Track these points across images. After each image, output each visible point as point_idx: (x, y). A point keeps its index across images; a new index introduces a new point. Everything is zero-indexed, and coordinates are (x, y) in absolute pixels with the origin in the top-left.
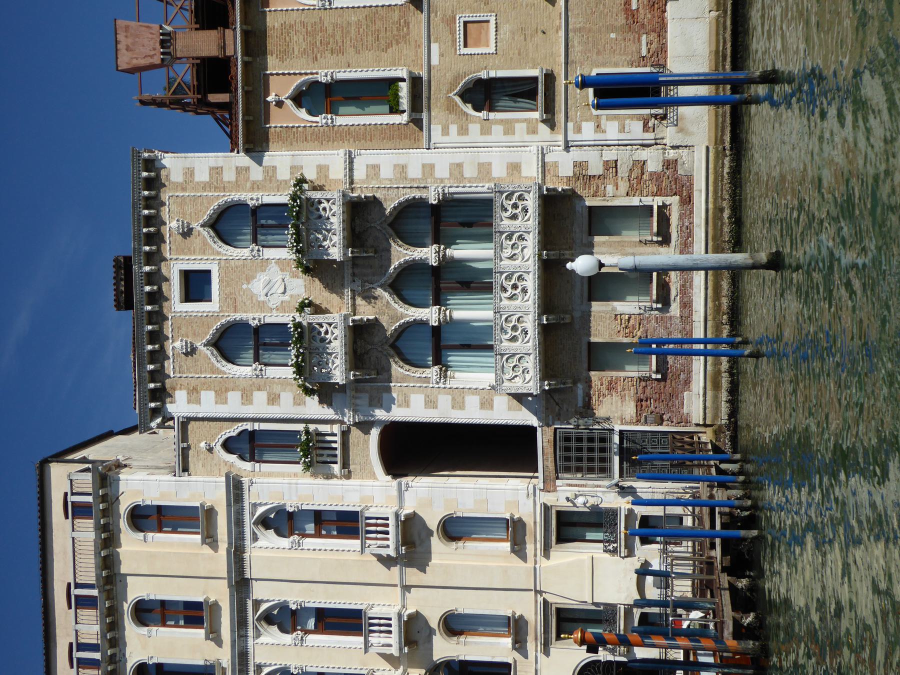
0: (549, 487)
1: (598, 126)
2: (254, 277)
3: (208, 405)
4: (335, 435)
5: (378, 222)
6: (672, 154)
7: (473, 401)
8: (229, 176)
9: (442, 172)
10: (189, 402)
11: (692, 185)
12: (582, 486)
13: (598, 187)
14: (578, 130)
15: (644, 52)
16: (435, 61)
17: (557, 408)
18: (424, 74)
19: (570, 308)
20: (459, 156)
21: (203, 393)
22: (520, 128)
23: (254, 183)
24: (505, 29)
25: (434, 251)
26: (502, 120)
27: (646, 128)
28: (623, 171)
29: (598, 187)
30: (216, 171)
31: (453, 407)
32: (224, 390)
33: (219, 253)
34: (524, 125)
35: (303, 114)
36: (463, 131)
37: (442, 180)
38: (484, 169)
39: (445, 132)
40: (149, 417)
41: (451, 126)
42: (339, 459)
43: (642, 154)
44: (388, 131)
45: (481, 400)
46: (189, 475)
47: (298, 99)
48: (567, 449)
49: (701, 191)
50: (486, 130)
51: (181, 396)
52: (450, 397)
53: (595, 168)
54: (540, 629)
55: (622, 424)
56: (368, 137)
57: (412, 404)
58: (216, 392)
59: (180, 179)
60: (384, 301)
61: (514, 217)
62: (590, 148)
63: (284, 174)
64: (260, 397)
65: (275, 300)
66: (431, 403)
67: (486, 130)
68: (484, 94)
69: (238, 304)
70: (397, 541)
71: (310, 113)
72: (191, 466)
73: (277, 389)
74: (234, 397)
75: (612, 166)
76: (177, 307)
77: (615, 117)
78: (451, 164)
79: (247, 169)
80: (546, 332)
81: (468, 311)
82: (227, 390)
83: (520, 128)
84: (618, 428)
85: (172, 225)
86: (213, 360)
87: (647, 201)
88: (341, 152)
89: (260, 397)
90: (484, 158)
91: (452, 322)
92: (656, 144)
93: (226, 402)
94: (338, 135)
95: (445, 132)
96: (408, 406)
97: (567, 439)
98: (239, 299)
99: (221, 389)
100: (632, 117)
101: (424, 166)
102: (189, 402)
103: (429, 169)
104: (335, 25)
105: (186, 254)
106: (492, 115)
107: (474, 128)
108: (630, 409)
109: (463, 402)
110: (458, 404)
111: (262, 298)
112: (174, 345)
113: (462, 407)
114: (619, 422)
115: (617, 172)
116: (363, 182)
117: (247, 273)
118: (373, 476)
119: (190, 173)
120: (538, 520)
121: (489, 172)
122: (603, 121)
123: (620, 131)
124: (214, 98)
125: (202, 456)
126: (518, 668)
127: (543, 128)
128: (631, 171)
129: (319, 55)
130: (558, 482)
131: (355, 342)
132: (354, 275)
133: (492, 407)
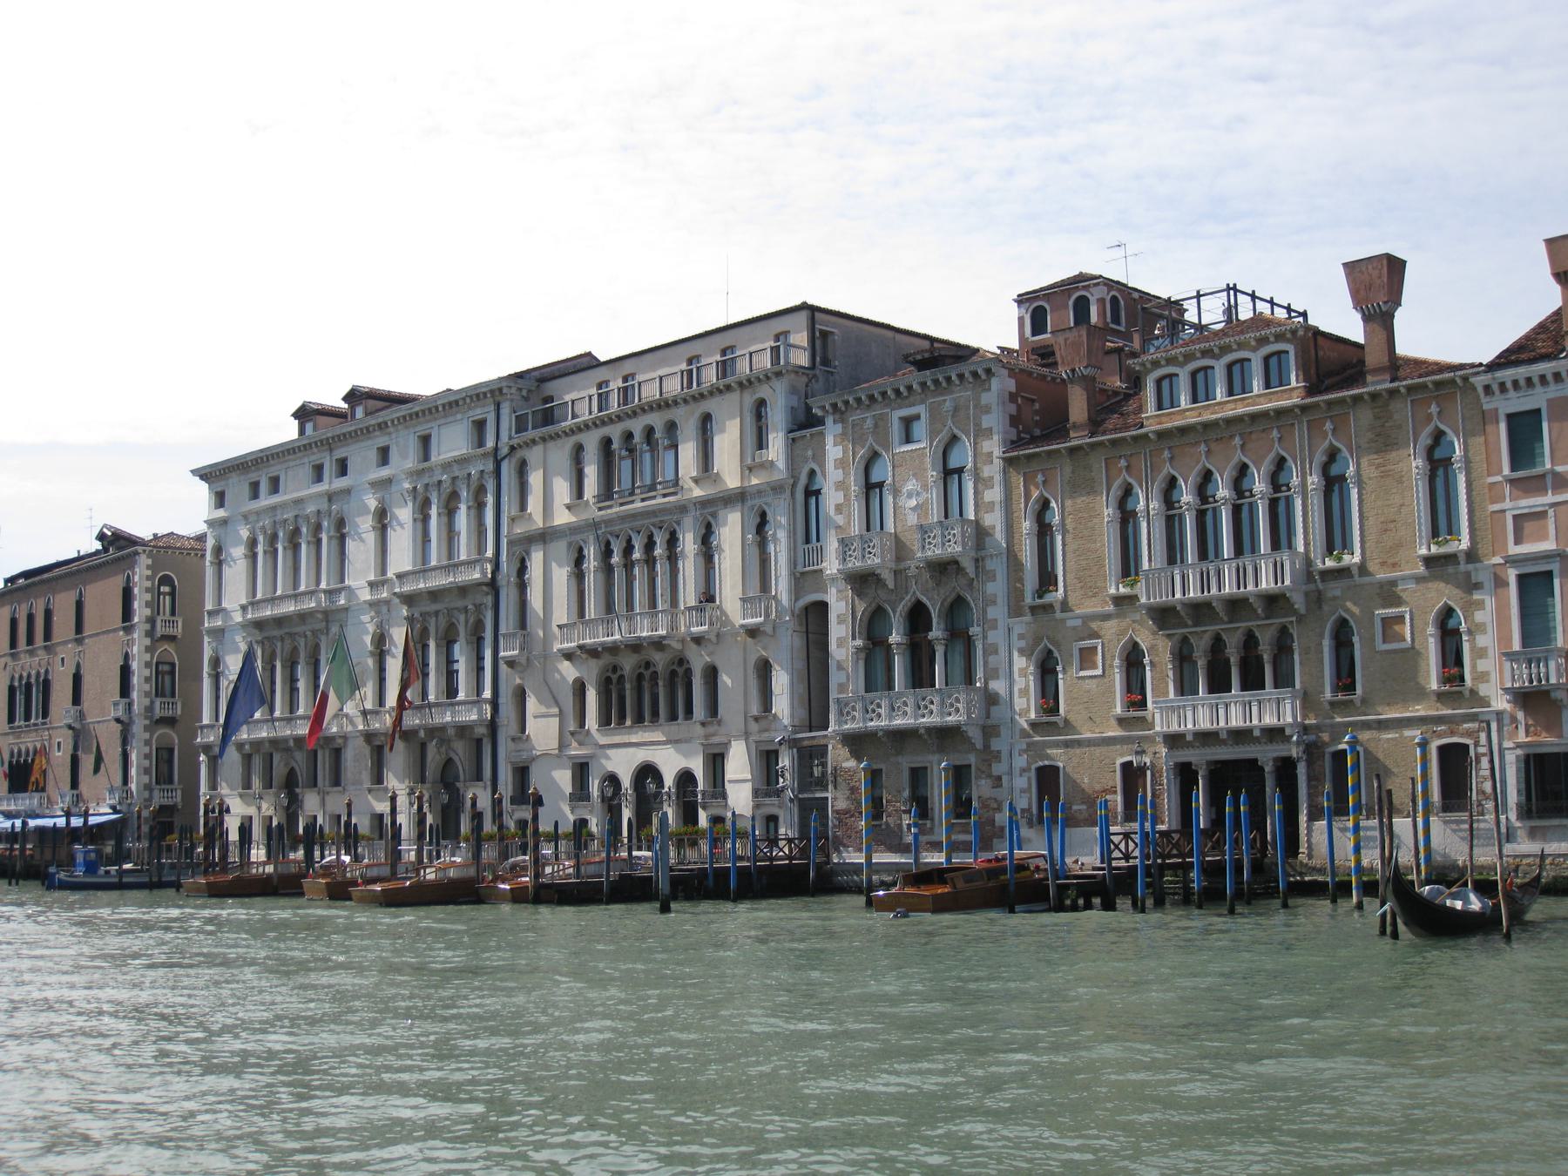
3: (833, 451)
24: (1092, 684)
27: (1023, 811)
28: (996, 793)
37: (985, 637)
39: (1021, 637)
51: (839, 428)
53: (997, 769)
59: (983, 402)
84: (829, 795)
95: (1021, 637)
103: (994, 625)
104: (1093, 529)
108: (842, 804)
117: (919, 475)
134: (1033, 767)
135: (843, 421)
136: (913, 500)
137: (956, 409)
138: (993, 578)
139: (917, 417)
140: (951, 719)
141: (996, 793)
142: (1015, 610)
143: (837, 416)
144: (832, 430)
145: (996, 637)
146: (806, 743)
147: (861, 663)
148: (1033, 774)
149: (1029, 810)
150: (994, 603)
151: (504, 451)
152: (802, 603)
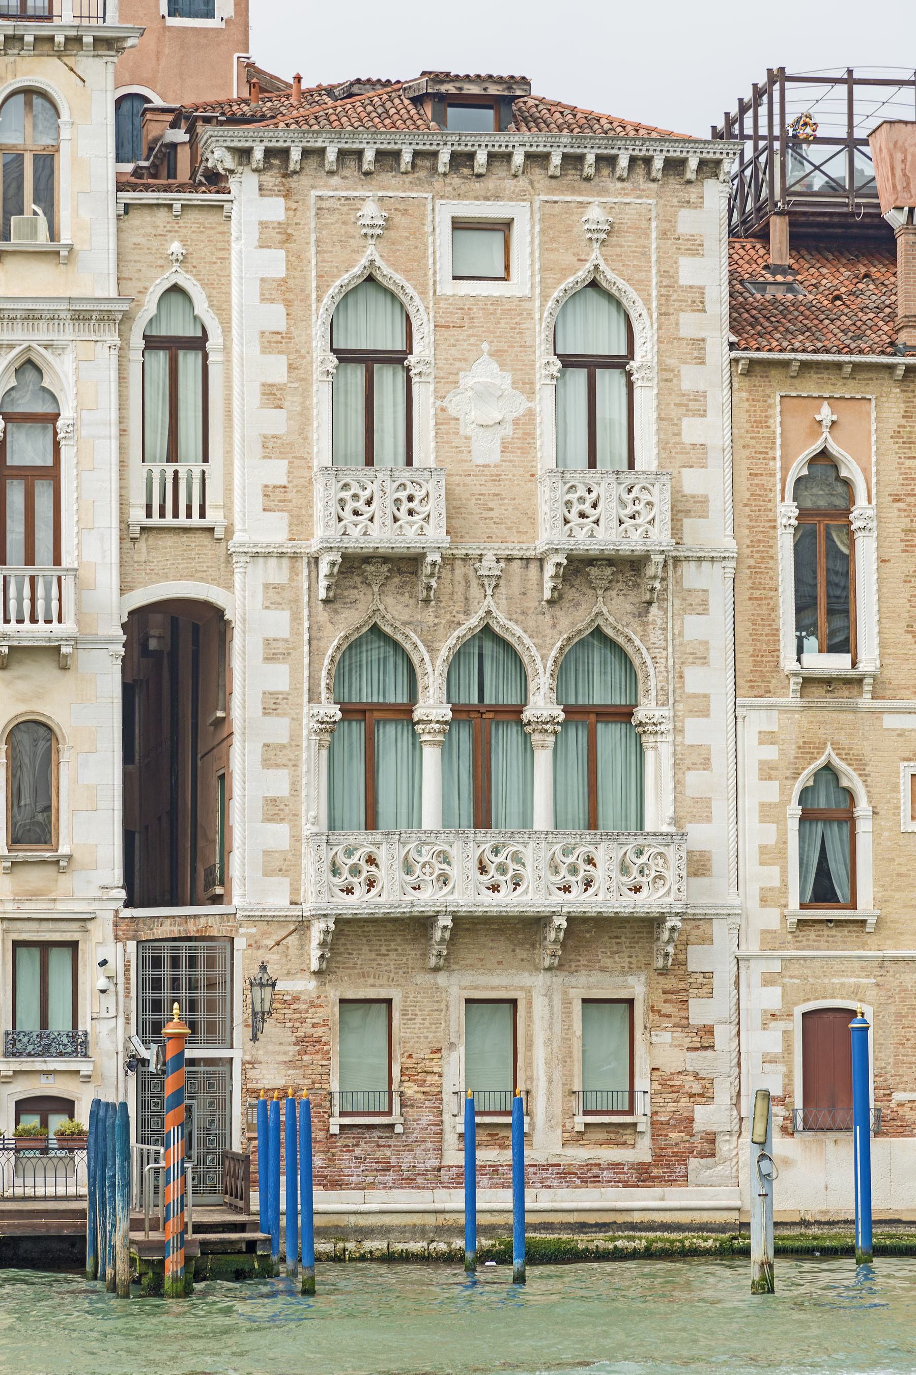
0: (123, 929)
1: (773, 1015)
2: (502, 366)
4: (202, 515)
5: (605, 610)
6: (724, 1147)
7: (278, 783)
8: (689, 324)
9: (696, 731)
10: (263, 225)
11: (671, 1182)
12: (127, 989)
13: (669, 1016)
14: (768, 980)
15: (899, 1096)
16: (890, 722)
17: (271, 943)
18: (866, 700)
19: (454, 967)
20: (721, 763)
21: (282, 253)
22: (771, 876)
23: (678, 376)
25: (555, 714)
26: (785, 843)
29: (669, 1016)
31: (267, 745)
32: (290, 296)
33: (545, 297)
34: (777, 883)
35: (798, 468)
36: (767, 771)
38: (701, 809)
39: (767, 738)
40: (235, 144)
41: (776, 747)
42: (156, 521)
43: (723, 1094)
44: (767, 630)
45: (282, 799)
46: (118, 216)
49: (663, 1199)
50: (768, 812)
51: (275, 209)
52: (285, 741)
53: (700, 1011)
55: (243, 1064)
56: (757, 593)
57: (271, 667)
58: (284, 280)
60: (461, 617)
61: (624, 869)
62: (735, 1000)
63: (693, 430)
64: (276, 369)
66: (273, 704)
67: (768, 812)
68: (827, 810)
69: (455, 332)
70: (20, 639)
72: (136, 219)
73: (292, 401)
74: (275, 317)
75: (704, 1039)
77: (788, 1048)
78: (709, 748)
79: (701, 361)
80: (419, 926)
82: (288, 303)
83: (771, 876)
84: (237, 1054)
87: (643, 1105)
88: (732, 544)
89: (276, 369)
90: (722, 808)
91: (416, 745)
92: (741, 1119)
93: (263, 300)
94: (760, 537)
95: (767, 738)
96: (267, 659)
97: (211, 963)
98: (461, 335)
99: (290, 290)
100: (789, 1076)
101: (706, 696)
103: (701, 706)
105: (543, 231)
106: (794, 825)
107: (771, 791)
108: (272, 1077)
109: (277, 766)
110: (272, 755)
113: (267, 763)
114: (248, 1058)
115: (697, 1049)
116: (678, 582)
118: (124, 589)
119: (695, 248)
120: (61, 906)
121: (695, 819)
122: (781, 1025)
123: (765, 1055)
124: (779, 229)
125: (155, 244)
127: (771, 919)
128: (696, 1075)
129: (901, 505)
130: (132, 945)
131: (386, 559)
132: (509, 559)
133: (268, 819)
134: (799, 1011)
135: (287, 195)
136: (485, 407)
138: (703, 608)
139: (505, 226)
140: (648, 902)
142: (755, 675)
143: (271, 179)
144: (251, 202)
146: (160, 933)
147: (324, 752)
148: (796, 1026)
150: (704, 660)
152: (141, 597)
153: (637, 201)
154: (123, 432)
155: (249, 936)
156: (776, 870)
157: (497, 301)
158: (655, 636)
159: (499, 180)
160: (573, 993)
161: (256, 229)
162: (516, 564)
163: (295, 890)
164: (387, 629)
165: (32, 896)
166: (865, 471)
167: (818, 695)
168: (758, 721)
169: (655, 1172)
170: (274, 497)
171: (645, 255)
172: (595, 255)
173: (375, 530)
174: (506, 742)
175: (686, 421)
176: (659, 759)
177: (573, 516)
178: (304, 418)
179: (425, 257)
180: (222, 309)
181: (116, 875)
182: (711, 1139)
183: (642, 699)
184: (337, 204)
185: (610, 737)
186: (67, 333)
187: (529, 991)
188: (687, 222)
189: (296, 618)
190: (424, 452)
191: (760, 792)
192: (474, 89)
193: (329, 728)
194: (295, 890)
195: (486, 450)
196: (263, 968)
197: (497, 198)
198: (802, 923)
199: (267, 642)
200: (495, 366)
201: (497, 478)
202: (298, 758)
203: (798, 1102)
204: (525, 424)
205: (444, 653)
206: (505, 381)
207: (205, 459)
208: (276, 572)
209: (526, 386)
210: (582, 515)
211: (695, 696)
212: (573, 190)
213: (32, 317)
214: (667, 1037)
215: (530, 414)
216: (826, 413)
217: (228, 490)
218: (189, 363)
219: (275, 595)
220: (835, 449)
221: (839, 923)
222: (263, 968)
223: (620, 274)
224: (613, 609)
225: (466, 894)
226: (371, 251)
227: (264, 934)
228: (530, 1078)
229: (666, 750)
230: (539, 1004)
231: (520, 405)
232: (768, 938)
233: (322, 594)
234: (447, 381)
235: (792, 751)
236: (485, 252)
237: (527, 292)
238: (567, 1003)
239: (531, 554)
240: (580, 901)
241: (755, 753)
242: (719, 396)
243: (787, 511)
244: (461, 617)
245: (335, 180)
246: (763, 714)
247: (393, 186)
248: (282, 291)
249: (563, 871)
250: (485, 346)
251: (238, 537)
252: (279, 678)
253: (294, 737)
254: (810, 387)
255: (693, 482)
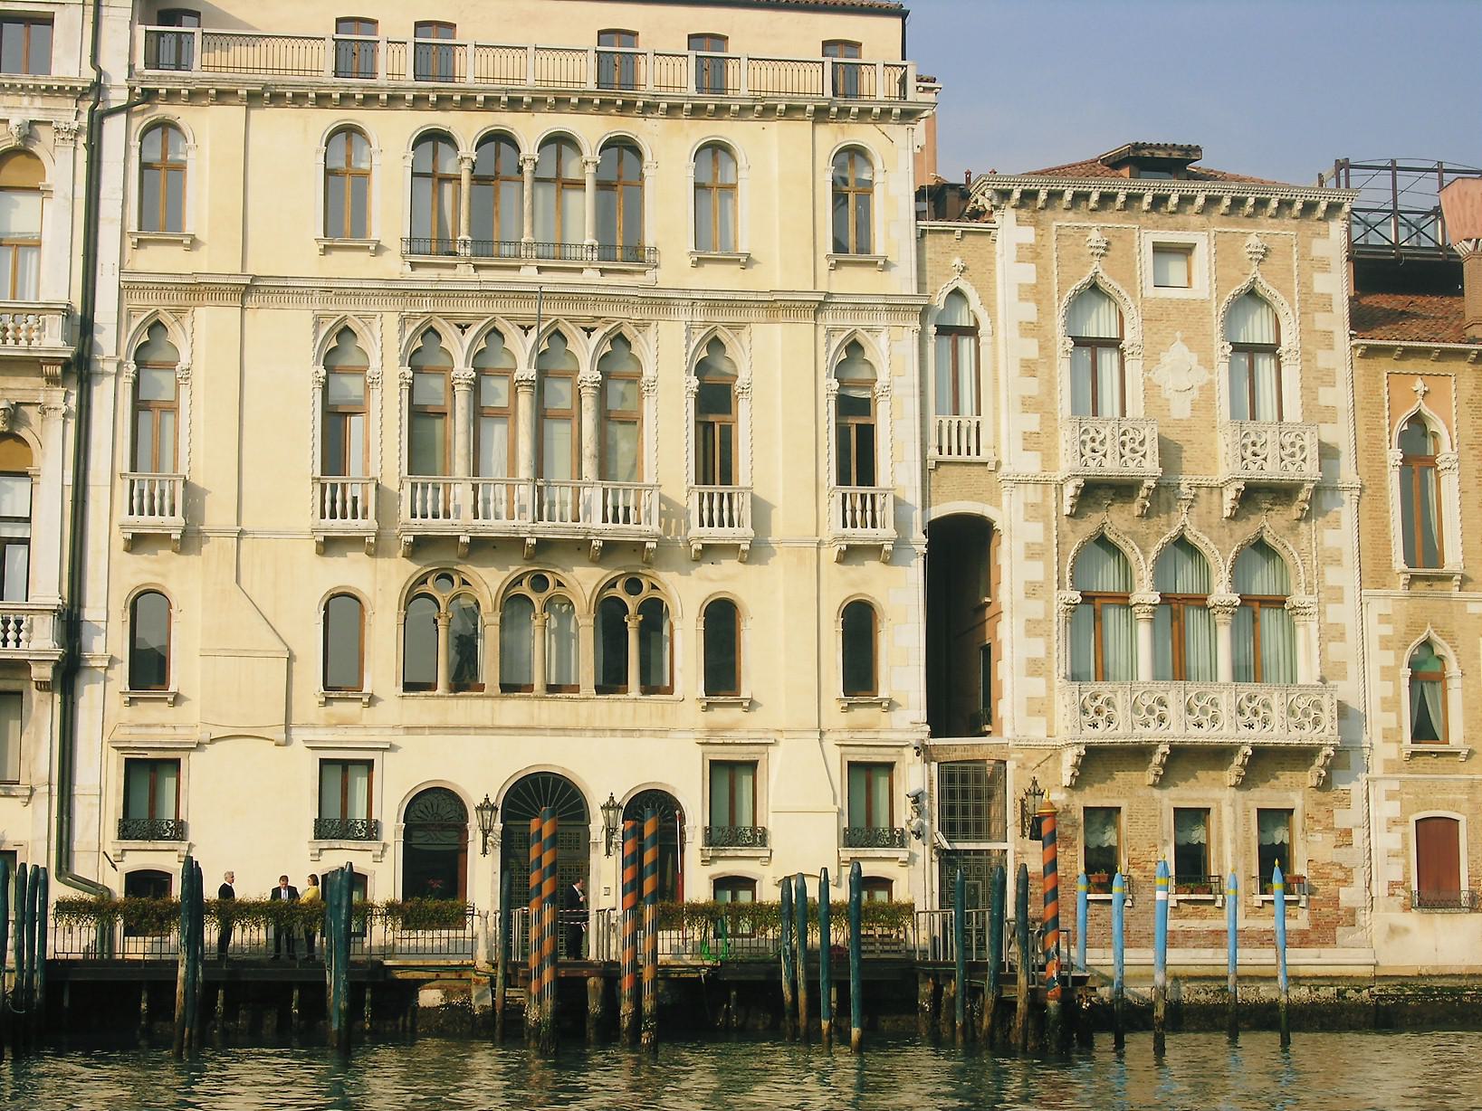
6: (1361, 918)
8: (1321, 321)
9: (1334, 613)
10: (1020, 246)
11: (1324, 944)
14: (1390, 796)
23: (1315, 357)
27: (1392, 885)
30: (1326, 304)
34: (1394, 725)
35: (1400, 424)
36: (1385, 643)
38: (1339, 670)
39: (1384, 619)
42: (945, 457)
43: (1359, 881)
47: (1417, 420)
48: (964, 779)
50: (1388, 673)
51: (1028, 235)
52: (1041, 617)
53: (1342, 819)
54: (730, 736)
60: (1165, 529)
63: (1326, 396)
64: (1031, 349)
65: (1163, 375)
66: (1032, 590)
71: (1402, 434)
74: (1029, 311)
76: (1150, 236)
77: (1406, 846)
79: (1331, 347)
81: (1139, 642)
82: (1038, 302)
85: (1254, 236)
86: (1077, 285)
89: (1031, 349)
90: (1353, 669)
95: (1384, 619)
101: (1341, 588)
102: (1020, 246)
103: (1337, 595)
107: (1389, 658)
109: (1036, 635)
110: (1033, 628)
111: (1166, 358)
112: (1095, 229)
118: (925, 505)
119: (1324, 266)
120: (882, 736)
122: (1400, 829)
126: (669, 707)
128: (1341, 867)
130: (934, 765)
134: (1413, 819)
135: (1036, 225)
137: (1267, 252)
139: (1186, 250)
141: (1341, 855)
142: (1374, 575)
143: (1024, 213)
144: (1010, 229)
145: (1342, 614)
149: (1402, 885)
151: (118, 97)
152: (937, 512)
153: (1281, 232)
154: (923, 393)
155: (1017, 760)
156: (1393, 716)
157: (1186, 302)
158: (1304, 544)
159: (1191, 216)
160: (1251, 804)
161: (1014, 248)
162: (1203, 492)
163: (1050, 726)
164: (1112, 537)
165: (860, 729)
166: (1448, 427)
167: (1420, 586)
168: (1377, 607)
169: (1312, 936)
170: (1031, 441)
171: (1290, 270)
172: (1254, 270)
173: (1107, 463)
174: (1194, 618)
175: (1321, 390)
176: (1307, 634)
177: (1248, 454)
178: (1050, 384)
179: (1134, 271)
180: (989, 304)
181: (922, 715)
182: (1352, 912)
183: (1293, 589)
184: (1071, 232)
185: (1269, 618)
186: (882, 321)
187: (1218, 802)
188: (1319, 248)
189: (1047, 528)
190: (1135, 407)
191: (1380, 658)
192: (1161, 154)
193: (1073, 609)
194: (1050, 726)
195: (1180, 408)
196: (1035, 783)
197: (1185, 229)
198: (1414, 754)
199: (1028, 545)
200: (1185, 349)
201: (1188, 429)
202: (1051, 630)
203: (1415, 887)
204: (1208, 389)
205: (1153, 555)
206: (1193, 358)
207: (979, 414)
208: (1032, 494)
209: (1208, 363)
210: (1255, 455)
211: (1332, 588)
212: (1238, 225)
213: (858, 308)
214: (1319, 837)
215: (1211, 383)
216: (1419, 385)
217: (996, 435)
218: (966, 344)
219: (1033, 512)
220: (1426, 411)
221: (1439, 754)
222: (1035, 783)
223: (1272, 284)
224: (1271, 523)
225: (1178, 730)
226: (1096, 265)
227: (1029, 759)
228: (1221, 867)
229: (1314, 626)
230: (1227, 812)
231: (1201, 376)
232: (1390, 766)
233: (1067, 510)
234: (1151, 358)
235: (1403, 629)
236: (1176, 268)
237: (1206, 296)
238: (1247, 812)
239: (1213, 483)
240: (1260, 736)
241: (1376, 630)
242: (1343, 372)
243: (1394, 455)
244: (1165, 529)
245: (1070, 214)
246: (1382, 601)
247: (1112, 219)
248: (1035, 293)
249: (1248, 713)
250: (1178, 334)
251: (1004, 469)
252: (1036, 571)
253: (1048, 613)
254: (1409, 366)
255: (1328, 434)
